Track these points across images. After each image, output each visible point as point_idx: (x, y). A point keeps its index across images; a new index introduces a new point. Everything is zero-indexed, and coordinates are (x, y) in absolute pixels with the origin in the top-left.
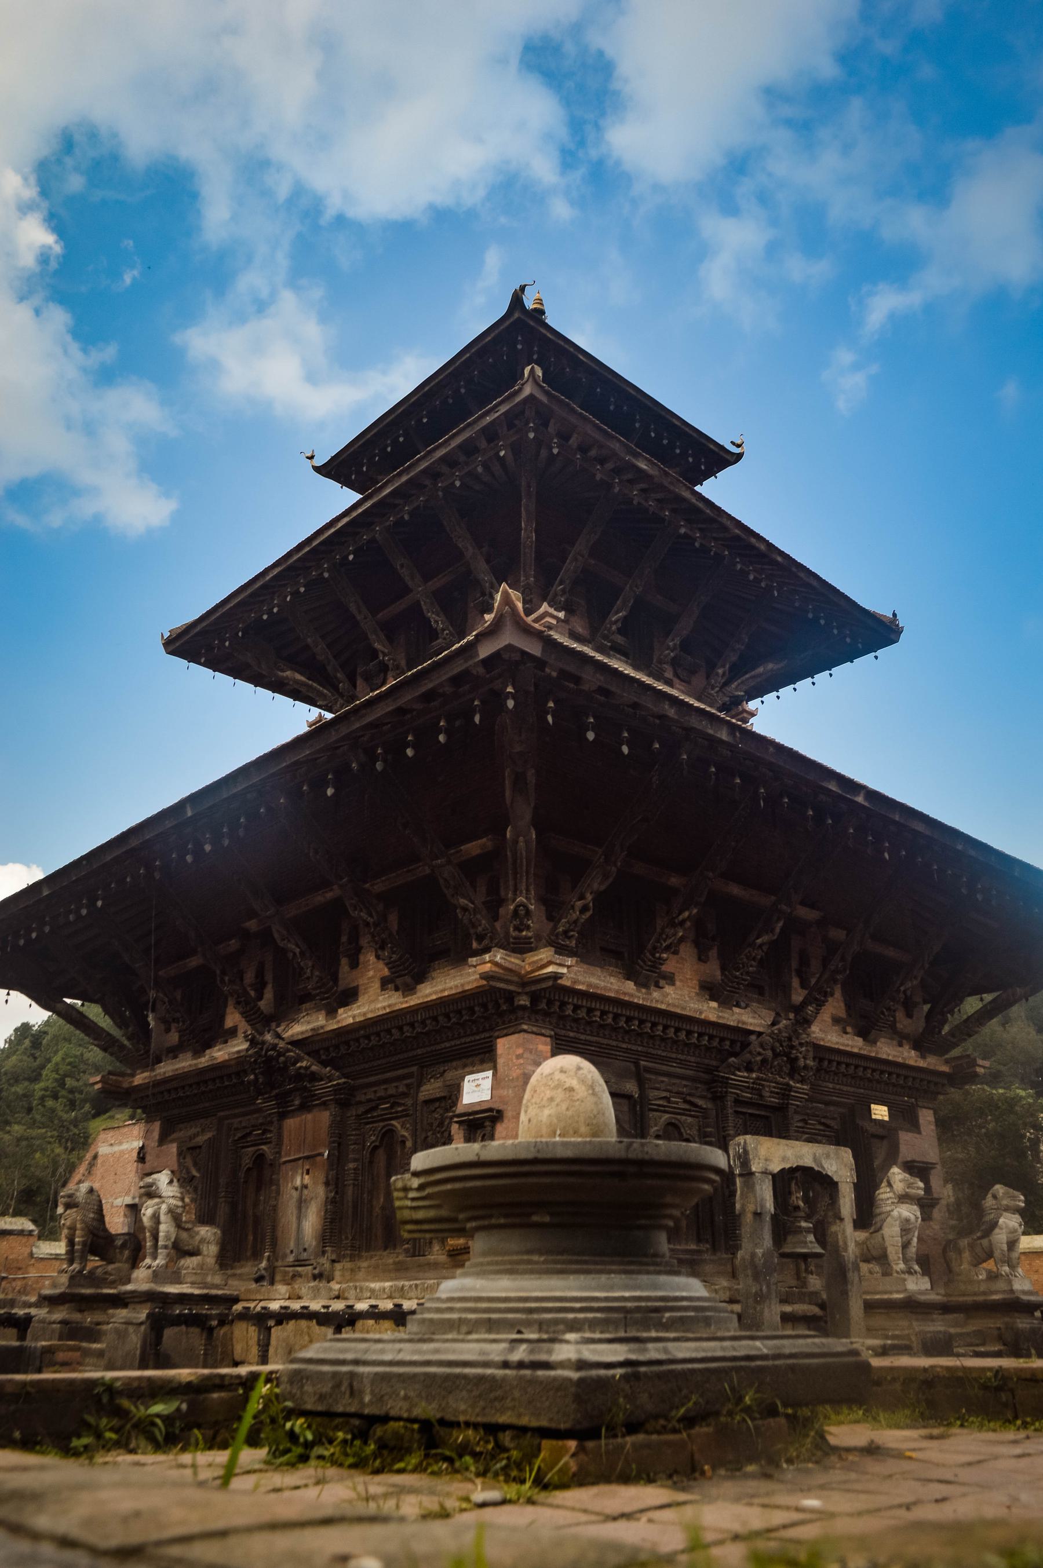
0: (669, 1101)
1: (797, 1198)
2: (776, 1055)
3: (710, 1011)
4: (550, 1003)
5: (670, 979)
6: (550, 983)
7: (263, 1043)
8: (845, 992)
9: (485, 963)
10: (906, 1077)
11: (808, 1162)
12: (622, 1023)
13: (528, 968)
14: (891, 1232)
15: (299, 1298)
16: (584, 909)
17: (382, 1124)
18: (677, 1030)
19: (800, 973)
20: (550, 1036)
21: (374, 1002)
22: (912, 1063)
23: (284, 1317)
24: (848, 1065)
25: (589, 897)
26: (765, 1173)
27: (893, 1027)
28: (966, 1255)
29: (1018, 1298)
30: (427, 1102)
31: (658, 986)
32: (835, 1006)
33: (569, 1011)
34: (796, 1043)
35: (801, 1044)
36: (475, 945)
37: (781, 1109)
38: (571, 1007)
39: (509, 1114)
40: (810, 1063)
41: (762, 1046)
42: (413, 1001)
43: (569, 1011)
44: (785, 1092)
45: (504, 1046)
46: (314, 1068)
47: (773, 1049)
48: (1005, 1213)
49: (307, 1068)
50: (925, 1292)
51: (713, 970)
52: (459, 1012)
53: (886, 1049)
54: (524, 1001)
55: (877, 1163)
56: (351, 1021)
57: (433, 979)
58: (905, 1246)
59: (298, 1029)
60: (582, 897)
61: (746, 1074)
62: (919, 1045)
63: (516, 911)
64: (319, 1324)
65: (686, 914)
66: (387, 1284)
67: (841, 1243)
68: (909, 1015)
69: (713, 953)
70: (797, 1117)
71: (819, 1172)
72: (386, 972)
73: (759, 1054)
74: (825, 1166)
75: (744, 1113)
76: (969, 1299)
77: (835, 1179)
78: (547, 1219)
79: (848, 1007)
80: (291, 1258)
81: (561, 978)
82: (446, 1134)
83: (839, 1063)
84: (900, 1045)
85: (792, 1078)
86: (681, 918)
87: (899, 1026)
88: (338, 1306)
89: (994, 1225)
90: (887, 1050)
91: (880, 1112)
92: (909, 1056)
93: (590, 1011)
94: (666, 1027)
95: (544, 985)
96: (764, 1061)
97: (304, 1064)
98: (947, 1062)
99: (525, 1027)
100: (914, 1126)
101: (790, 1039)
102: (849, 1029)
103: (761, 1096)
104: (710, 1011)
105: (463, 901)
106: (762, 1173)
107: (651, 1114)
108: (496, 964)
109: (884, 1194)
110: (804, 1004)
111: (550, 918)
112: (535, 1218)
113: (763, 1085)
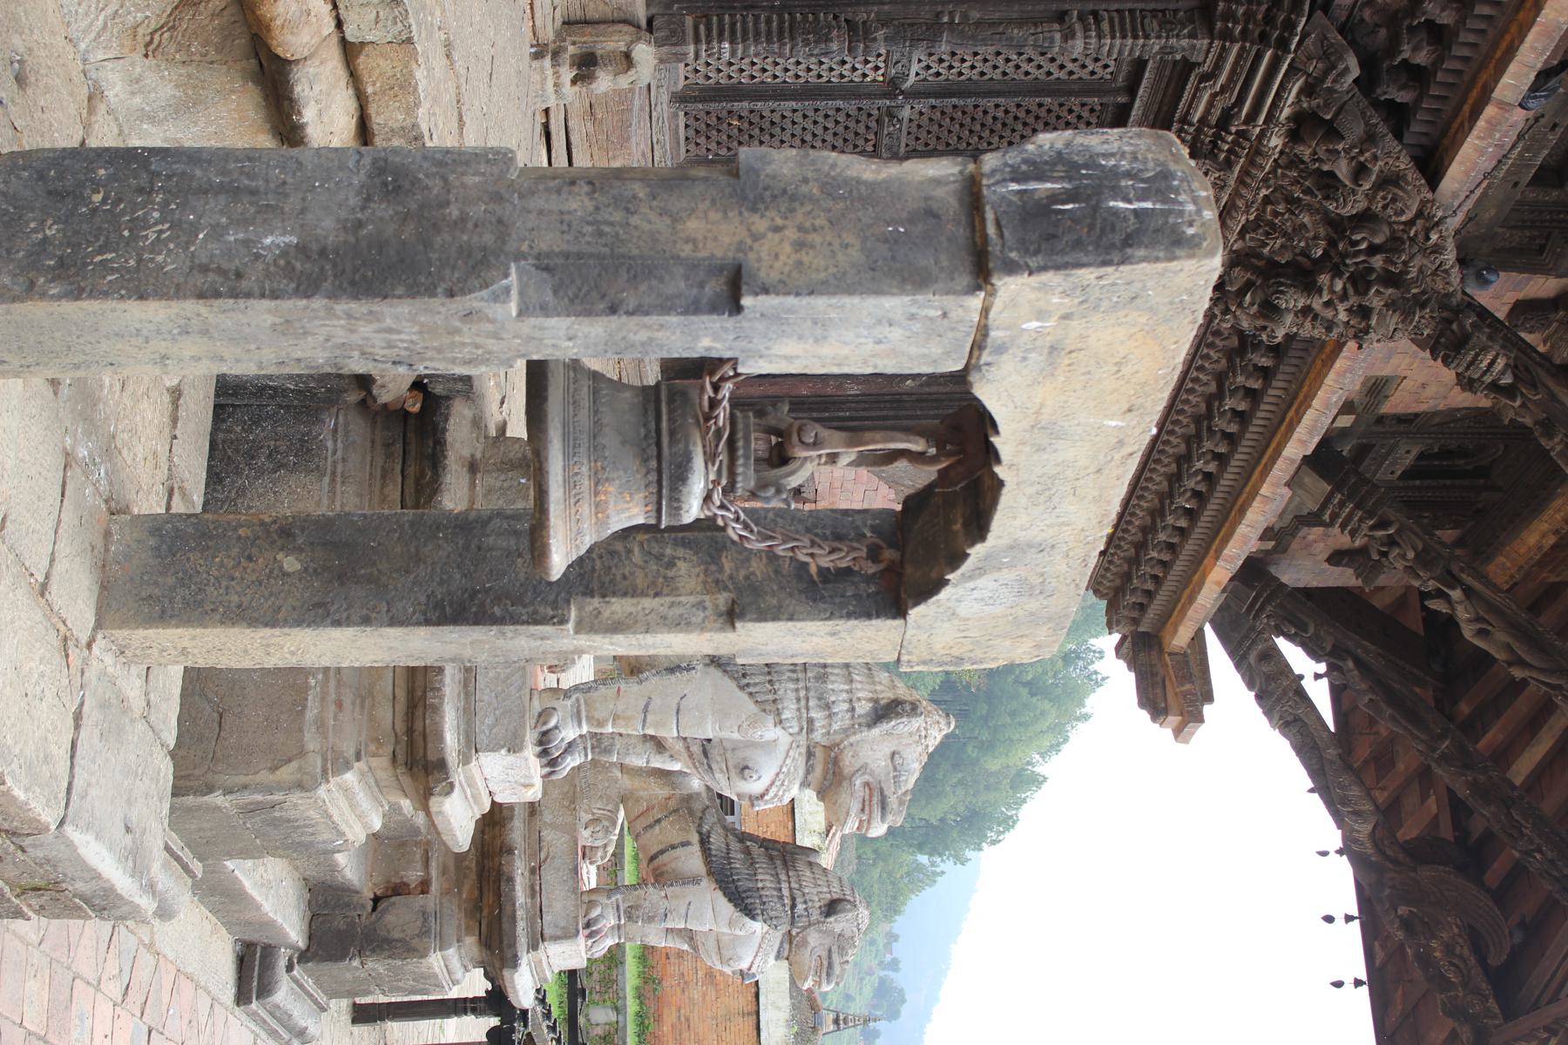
2: (1338, 227)
8: (1450, 419)
24: (1241, 417)
27: (1313, 519)
29: (514, 963)
41: (1390, 181)
47: (1365, 219)
48: (777, 937)
61: (1286, 112)
67: (619, 607)
74: (985, 583)
75: (1132, 89)
89: (744, 902)
96: (1328, 183)
102: (1346, 421)
106: (983, 330)
113: (1228, 164)
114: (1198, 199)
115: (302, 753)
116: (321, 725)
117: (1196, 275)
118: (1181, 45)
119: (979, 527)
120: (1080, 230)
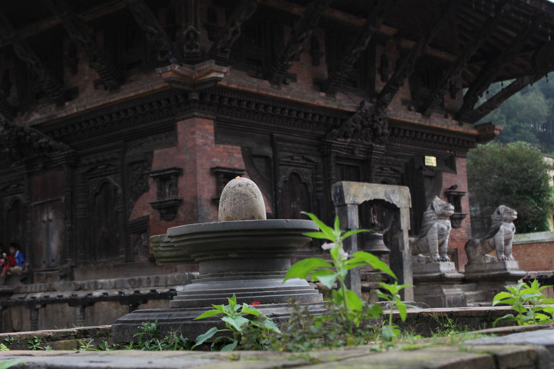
0: (292, 158)
1: (374, 219)
2: (363, 127)
3: (320, 99)
4: (212, 97)
5: (294, 78)
6: (212, 84)
7: (14, 127)
9: (167, 72)
10: (449, 138)
11: (381, 196)
12: (261, 109)
13: (197, 75)
14: (433, 236)
15: (54, 290)
16: (235, 32)
17: (100, 179)
18: (298, 112)
19: (381, 71)
20: (213, 119)
21: (90, 98)
22: (453, 128)
23: (45, 302)
24: (411, 132)
25: (238, 24)
26: (353, 204)
27: (442, 105)
28: (479, 248)
29: (508, 273)
30: (131, 164)
31: (285, 83)
32: (404, 92)
33: (226, 102)
34: (377, 118)
35: (380, 119)
36: (159, 58)
37: (366, 162)
38: (227, 100)
39: (187, 169)
40: (386, 131)
41: (354, 121)
42: (118, 97)
43: (226, 102)
44: (369, 151)
45: (181, 126)
46: (51, 143)
47: (362, 123)
48: (504, 223)
49: (46, 143)
50: (452, 271)
51: (324, 71)
52: (151, 104)
53: (436, 120)
54: (195, 96)
55: (427, 194)
56: (75, 111)
57: (131, 81)
58: (441, 245)
59: (36, 117)
60: (233, 25)
61: (343, 140)
62: (459, 117)
63: (188, 36)
64: (70, 305)
65: (304, 35)
66: (113, 280)
67: (400, 245)
68: (453, 97)
69: (323, 59)
70: (377, 166)
71: (388, 203)
72: (97, 77)
73: (353, 126)
74: (392, 198)
75: (342, 165)
76: (480, 275)
77: (398, 206)
78: (236, 256)
79: (413, 93)
80: (44, 266)
81: (220, 81)
82: (145, 185)
83: (405, 131)
84: (446, 117)
85: (373, 141)
86: (301, 37)
87: (446, 104)
88: (81, 294)
89: (497, 230)
90: (438, 122)
91: (431, 161)
92: (451, 125)
93: (240, 102)
94: (290, 111)
95: (208, 86)
96: (356, 131)
97: (44, 140)
98: (476, 127)
99: (196, 114)
100: (453, 169)
101: (373, 116)
102: (413, 108)
103: (353, 153)
104: (320, 99)
105: (151, 29)
106: (352, 204)
107: (281, 168)
108: (175, 72)
109: (429, 213)
110: (384, 92)
111: (211, 38)
112: (230, 256)
113: (355, 147)
114: (338, 183)
115: (440, 297)
116: (436, 294)
117: (344, 183)
118: (332, 159)
119: (383, 201)
120: (341, 196)
